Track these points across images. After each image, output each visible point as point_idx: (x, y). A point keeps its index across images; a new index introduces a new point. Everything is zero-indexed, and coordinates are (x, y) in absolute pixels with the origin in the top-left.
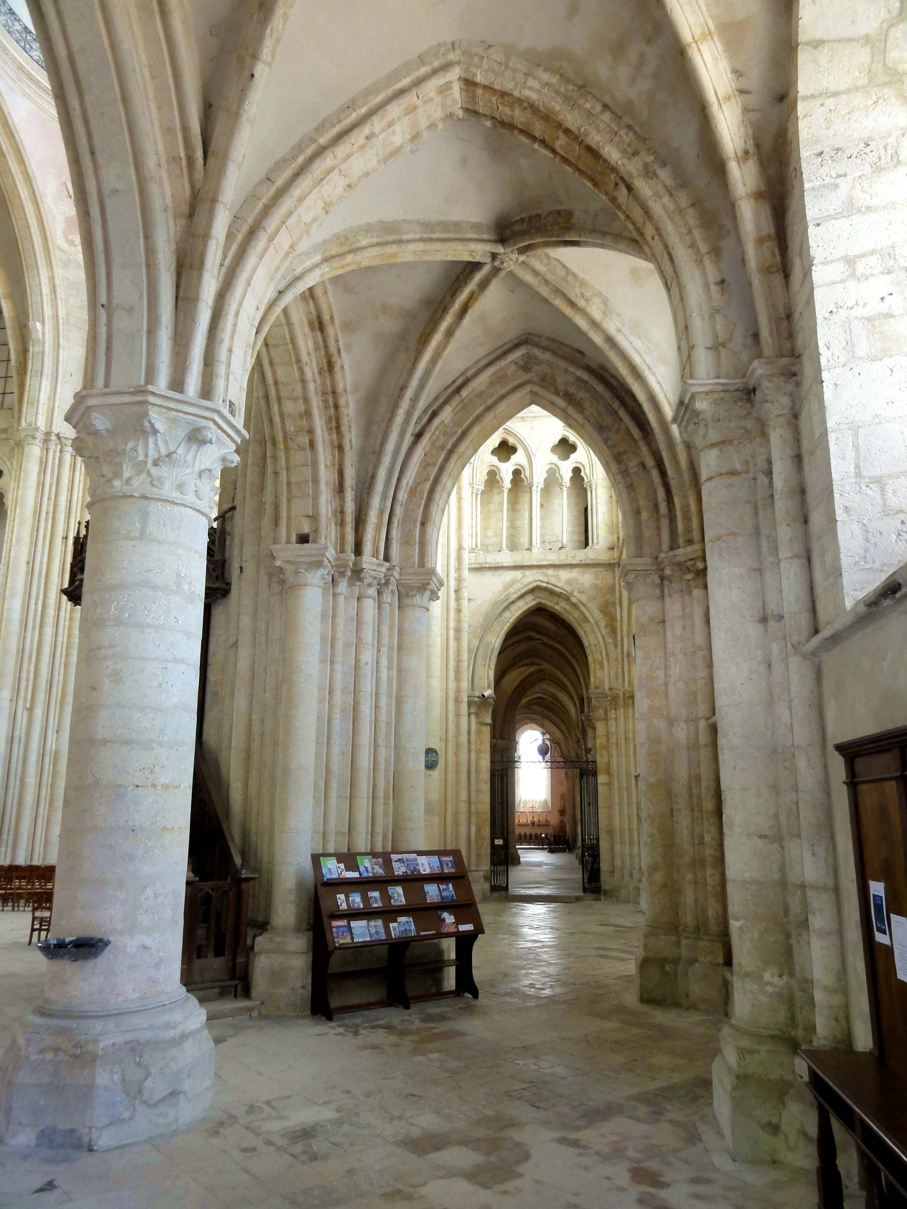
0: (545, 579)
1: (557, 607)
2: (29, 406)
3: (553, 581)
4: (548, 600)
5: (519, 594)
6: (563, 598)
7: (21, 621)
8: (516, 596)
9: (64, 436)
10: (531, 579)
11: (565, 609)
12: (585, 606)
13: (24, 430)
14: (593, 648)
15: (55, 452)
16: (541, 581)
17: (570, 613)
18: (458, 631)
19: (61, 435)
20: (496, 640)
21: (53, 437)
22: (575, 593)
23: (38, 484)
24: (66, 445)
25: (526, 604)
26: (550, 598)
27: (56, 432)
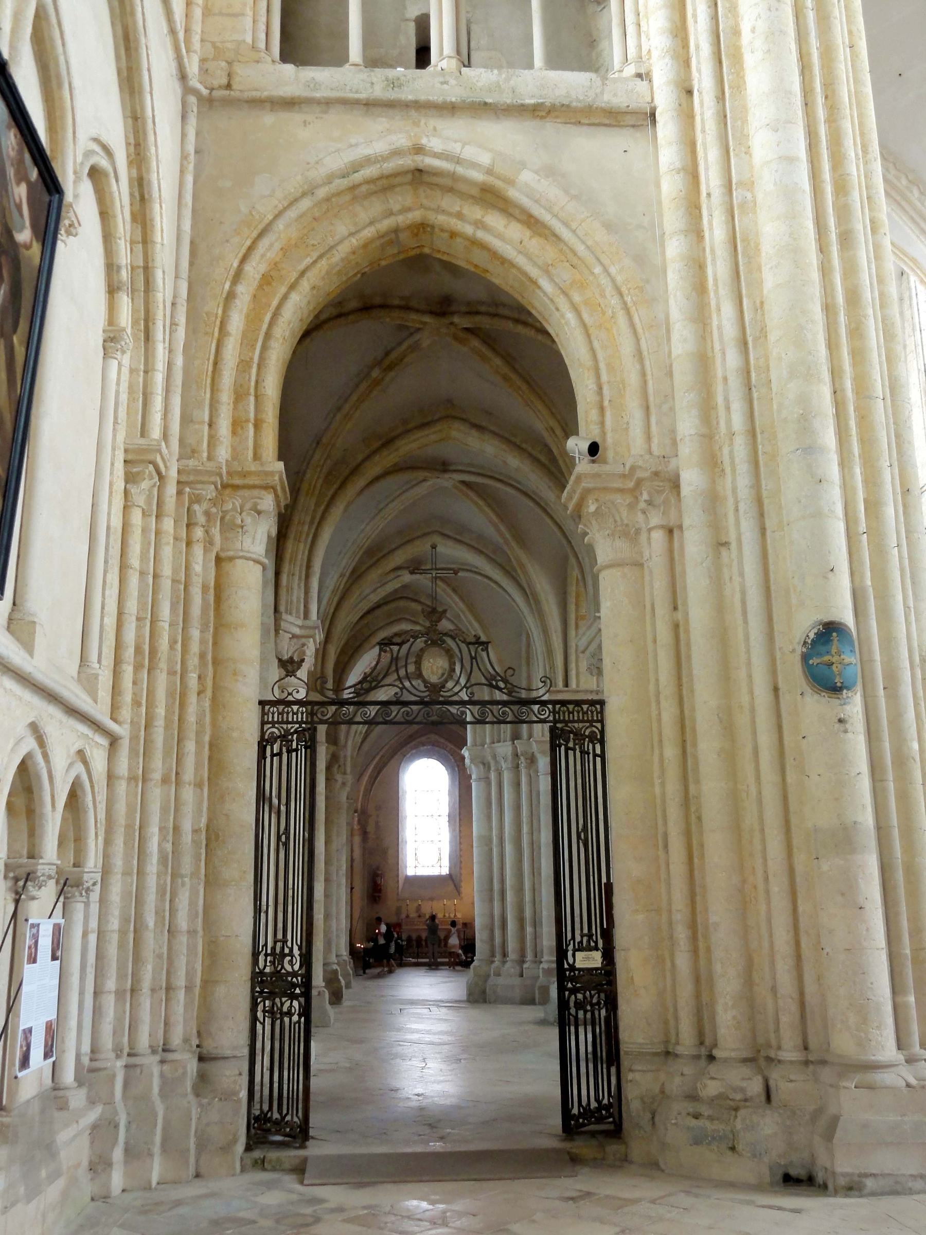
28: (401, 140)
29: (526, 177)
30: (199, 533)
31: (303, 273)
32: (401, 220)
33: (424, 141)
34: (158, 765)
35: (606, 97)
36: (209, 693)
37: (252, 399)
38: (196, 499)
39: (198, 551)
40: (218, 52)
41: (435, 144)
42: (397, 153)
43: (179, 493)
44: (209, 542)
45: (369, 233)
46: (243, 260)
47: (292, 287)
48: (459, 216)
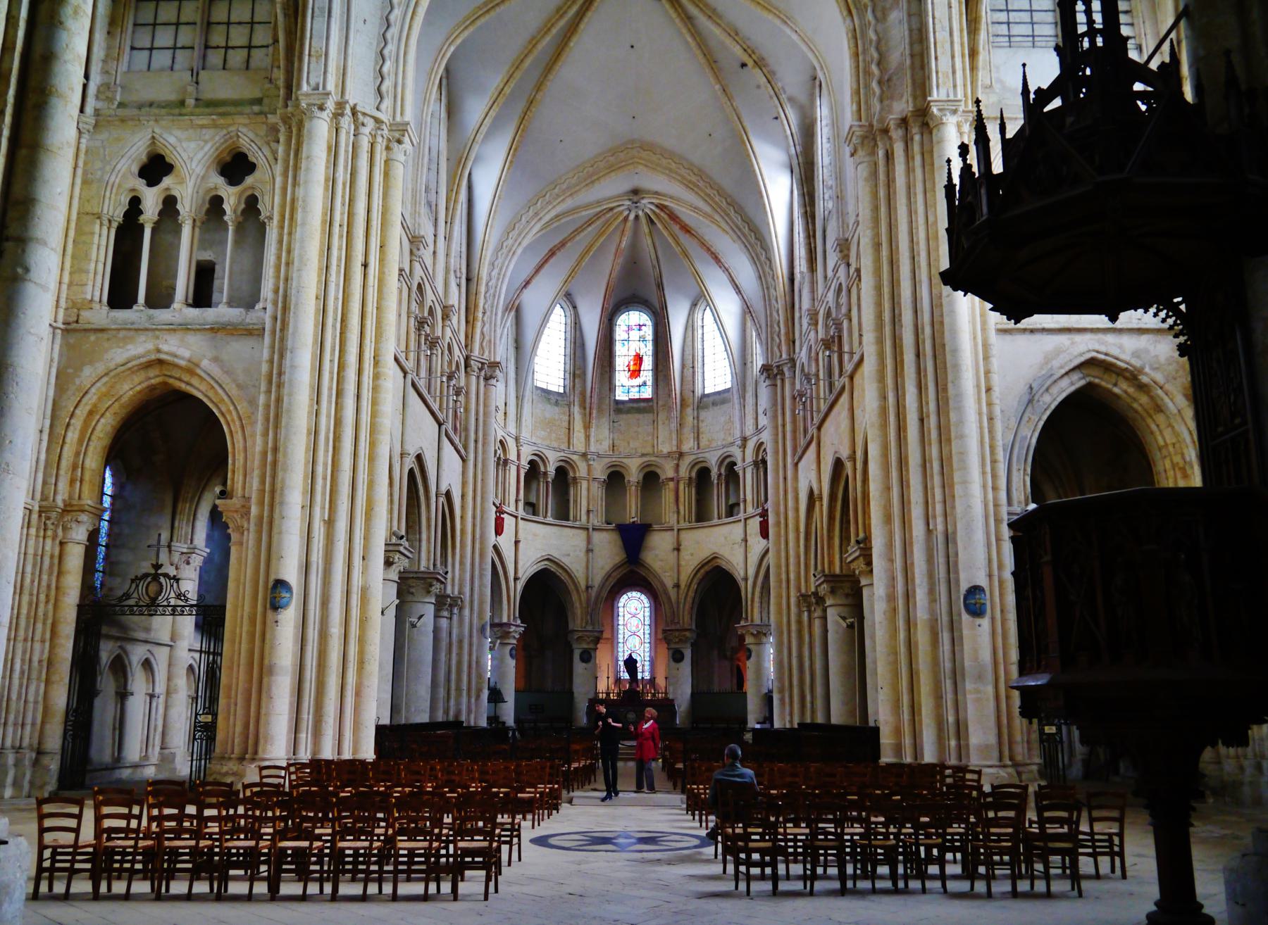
0: (1103, 349)
1: (1116, 390)
2: (313, 60)
3: (1115, 351)
4: (1101, 379)
5: (1067, 369)
6: (1126, 378)
7: (312, 387)
8: (1063, 371)
9: (363, 110)
10: (1082, 348)
11: (1126, 392)
12: (1161, 388)
13: (307, 95)
14: (1171, 449)
15: (348, 133)
16: (1098, 352)
17: (1135, 400)
18: (991, 419)
19: (358, 108)
20: (1031, 435)
21: (348, 111)
22: (1147, 370)
23: (327, 180)
24: (363, 125)
25: (1072, 384)
26: (1106, 377)
27: (352, 103)
28: (150, 346)
29: (205, 363)
30: (49, 533)
31: (108, 408)
32: (153, 381)
33: (160, 346)
34: (21, 633)
35: (248, 320)
36: (52, 601)
37: (80, 470)
38: (48, 518)
39: (49, 542)
40: (74, 304)
41: (165, 348)
42: (149, 351)
43: (40, 516)
44: (54, 538)
45: (138, 388)
46: (76, 408)
47: (102, 415)
48: (180, 380)
